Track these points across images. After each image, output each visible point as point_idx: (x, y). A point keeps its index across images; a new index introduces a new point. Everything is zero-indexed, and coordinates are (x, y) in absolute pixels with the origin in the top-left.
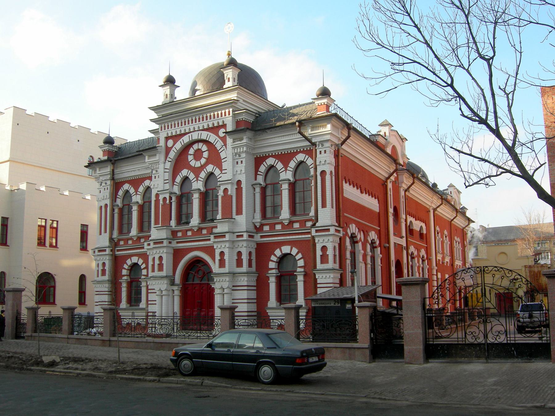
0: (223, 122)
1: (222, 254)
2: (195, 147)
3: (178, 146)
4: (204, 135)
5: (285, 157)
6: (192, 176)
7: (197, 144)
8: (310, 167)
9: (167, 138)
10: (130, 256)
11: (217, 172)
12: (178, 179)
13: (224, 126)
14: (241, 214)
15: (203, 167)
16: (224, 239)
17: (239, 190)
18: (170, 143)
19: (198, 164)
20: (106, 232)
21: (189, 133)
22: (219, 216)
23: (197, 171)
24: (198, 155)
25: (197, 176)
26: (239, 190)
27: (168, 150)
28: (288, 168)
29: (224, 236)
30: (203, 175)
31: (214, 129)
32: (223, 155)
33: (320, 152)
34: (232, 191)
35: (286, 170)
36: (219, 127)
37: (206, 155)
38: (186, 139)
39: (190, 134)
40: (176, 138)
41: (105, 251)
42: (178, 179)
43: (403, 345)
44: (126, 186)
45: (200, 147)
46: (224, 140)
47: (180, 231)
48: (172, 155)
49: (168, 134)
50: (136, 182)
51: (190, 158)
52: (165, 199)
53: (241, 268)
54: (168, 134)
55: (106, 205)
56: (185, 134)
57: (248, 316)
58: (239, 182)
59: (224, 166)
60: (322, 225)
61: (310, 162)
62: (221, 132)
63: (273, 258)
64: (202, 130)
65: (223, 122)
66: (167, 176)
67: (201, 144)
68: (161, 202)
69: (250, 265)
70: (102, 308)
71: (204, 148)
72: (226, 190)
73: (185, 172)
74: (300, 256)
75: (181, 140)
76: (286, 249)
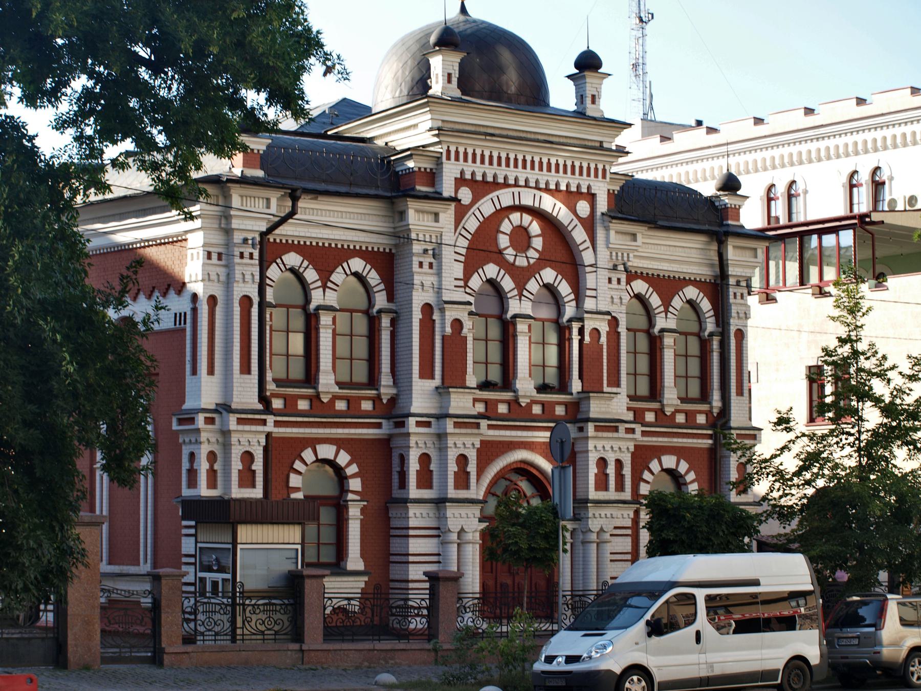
0: (589, 187)
1: (602, 462)
2: (515, 217)
3: (487, 207)
4: (548, 203)
5: (667, 286)
6: (507, 284)
7: (518, 214)
8: (707, 315)
9: (461, 181)
10: (313, 443)
11: (564, 289)
12: (476, 282)
13: (591, 197)
14: (618, 385)
15: (531, 271)
16: (615, 435)
17: (614, 334)
18: (465, 195)
19: (521, 262)
20: (246, 369)
21: (509, 186)
22: (576, 385)
23: (521, 277)
24: (521, 238)
25: (521, 287)
26: (614, 334)
27: (461, 212)
28: (671, 309)
29: (616, 429)
30: (533, 286)
31: (570, 197)
32: (588, 257)
33: (735, 294)
34: (603, 339)
35: (666, 311)
36: (579, 194)
37: (538, 243)
38: (506, 198)
39: (516, 190)
40: (482, 187)
41: (264, 422)
42: (476, 282)
43: (794, 629)
44: (292, 259)
45: (525, 223)
46: (589, 224)
47: (503, 401)
48: (472, 223)
49: (462, 173)
50: (326, 258)
51: (504, 241)
52: (457, 324)
53: (622, 494)
54: (462, 173)
55: (246, 301)
56: (506, 185)
57: (408, 589)
58: (614, 323)
59: (590, 280)
60: (741, 425)
61: (706, 305)
62: (583, 208)
63: (647, 475)
64: (540, 189)
65: (589, 187)
66: (458, 270)
67: (527, 218)
68: (443, 326)
69: (620, 487)
70: (425, 574)
71: (535, 228)
72: (596, 332)
73: (491, 270)
74: (691, 476)
75: (493, 195)
76: (669, 461)
